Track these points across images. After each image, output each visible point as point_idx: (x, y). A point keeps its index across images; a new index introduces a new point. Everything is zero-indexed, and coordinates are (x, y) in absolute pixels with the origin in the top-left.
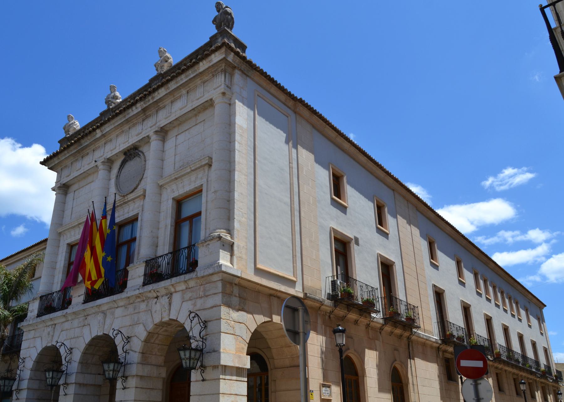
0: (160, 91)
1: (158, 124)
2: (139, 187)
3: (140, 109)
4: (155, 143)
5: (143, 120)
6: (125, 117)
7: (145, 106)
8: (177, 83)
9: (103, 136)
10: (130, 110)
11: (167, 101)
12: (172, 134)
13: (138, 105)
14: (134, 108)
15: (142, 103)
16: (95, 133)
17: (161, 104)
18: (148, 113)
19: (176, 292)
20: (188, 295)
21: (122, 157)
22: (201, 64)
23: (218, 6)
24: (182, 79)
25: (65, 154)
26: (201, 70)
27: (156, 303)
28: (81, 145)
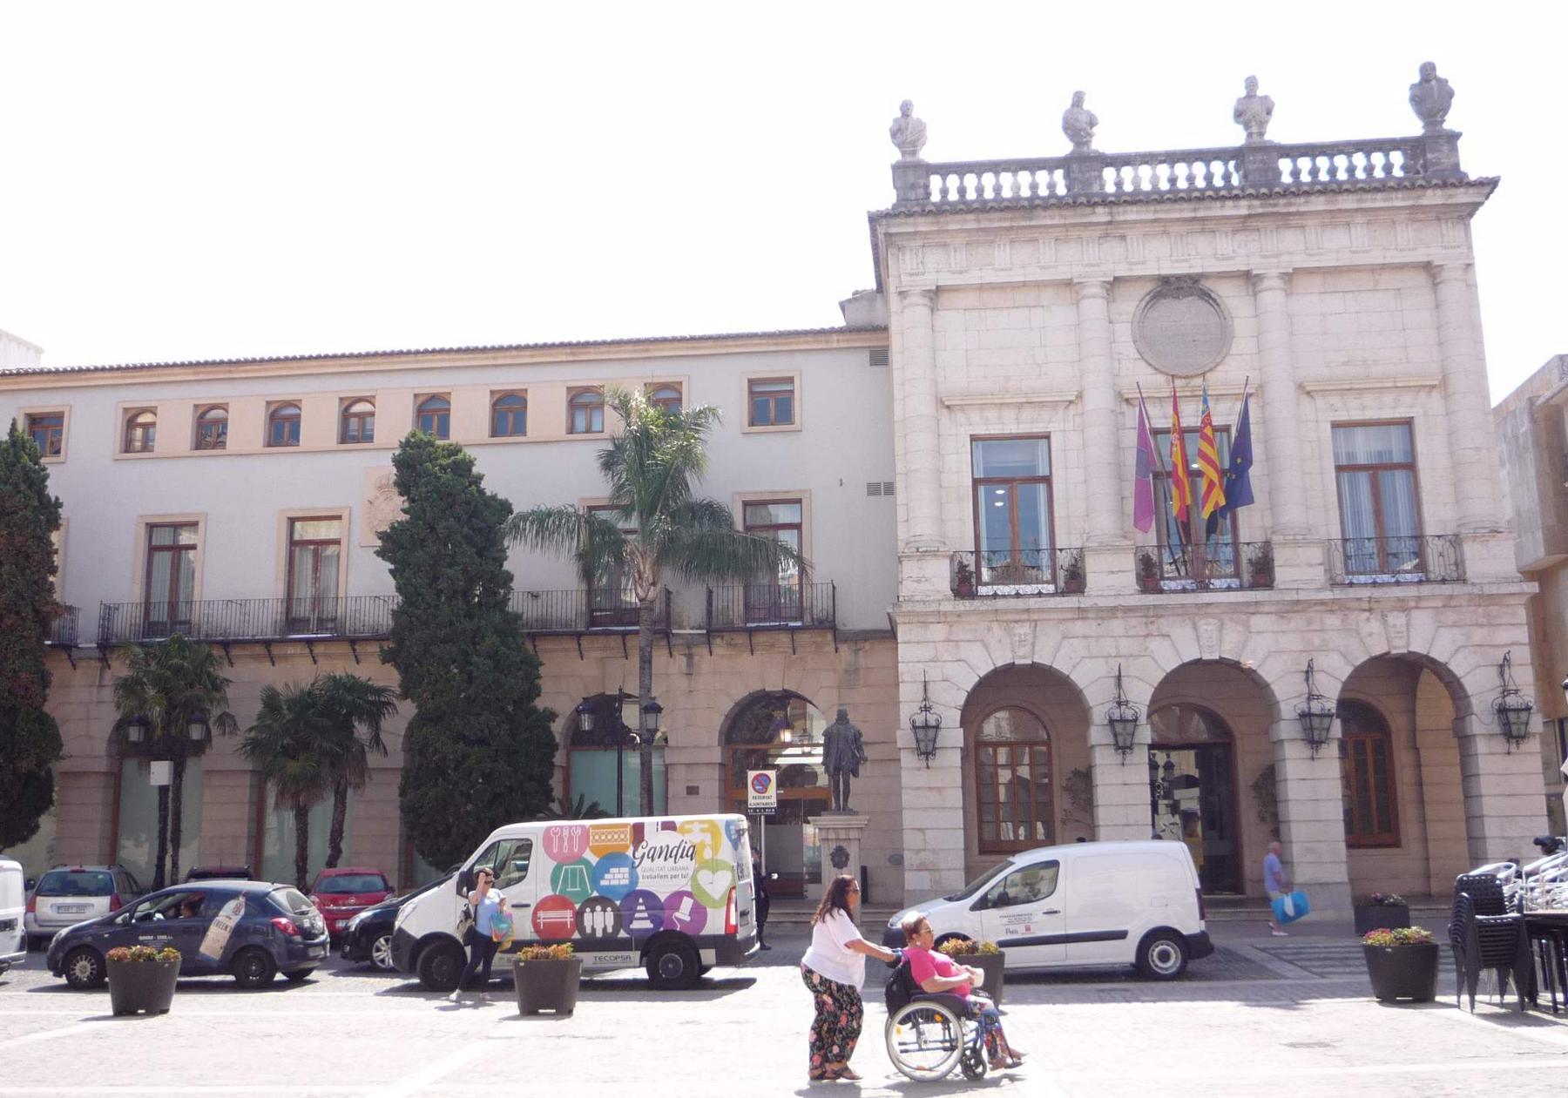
0: (1313, 198)
1: (1285, 258)
2: (1220, 368)
3: (1244, 212)
4: (1272, 297)
5: (1235, 232)
6: (1195, 210)
7: (1260, 211)
8: (1360, 201)
9: (1110, 223)
10: (1218, 204)
11: (1309, 222)
12: (1302, 282)
13: (1244, 203)
14: (1230, 203)
15: (1256, 203)
16: (1089, 210)
17: (1294, 221)
18: (1254, 223)
19: (1417, 608)
20: (1451, 617)
21: (1149, 287)
22: (1429, 192)
23: (1428, 71)
24: (1373, 200)
25: (965, 221)
26: (1425, 202)
27: (1368, 619)
28: (1031, 219)
